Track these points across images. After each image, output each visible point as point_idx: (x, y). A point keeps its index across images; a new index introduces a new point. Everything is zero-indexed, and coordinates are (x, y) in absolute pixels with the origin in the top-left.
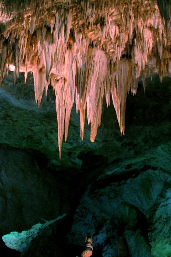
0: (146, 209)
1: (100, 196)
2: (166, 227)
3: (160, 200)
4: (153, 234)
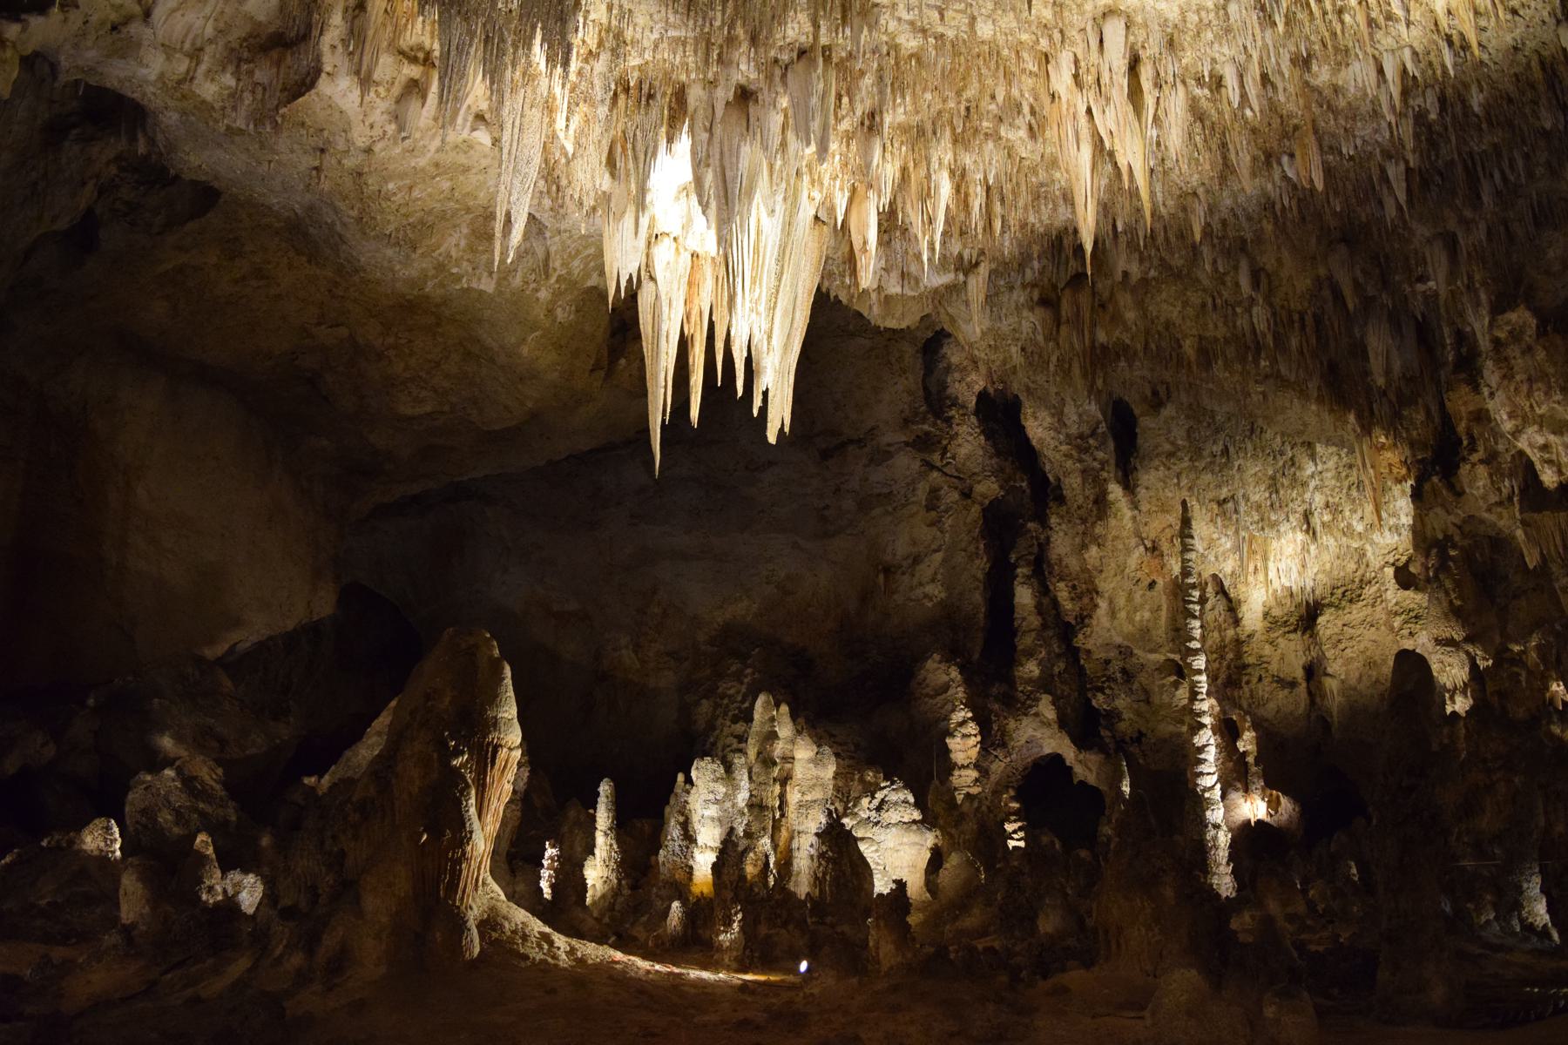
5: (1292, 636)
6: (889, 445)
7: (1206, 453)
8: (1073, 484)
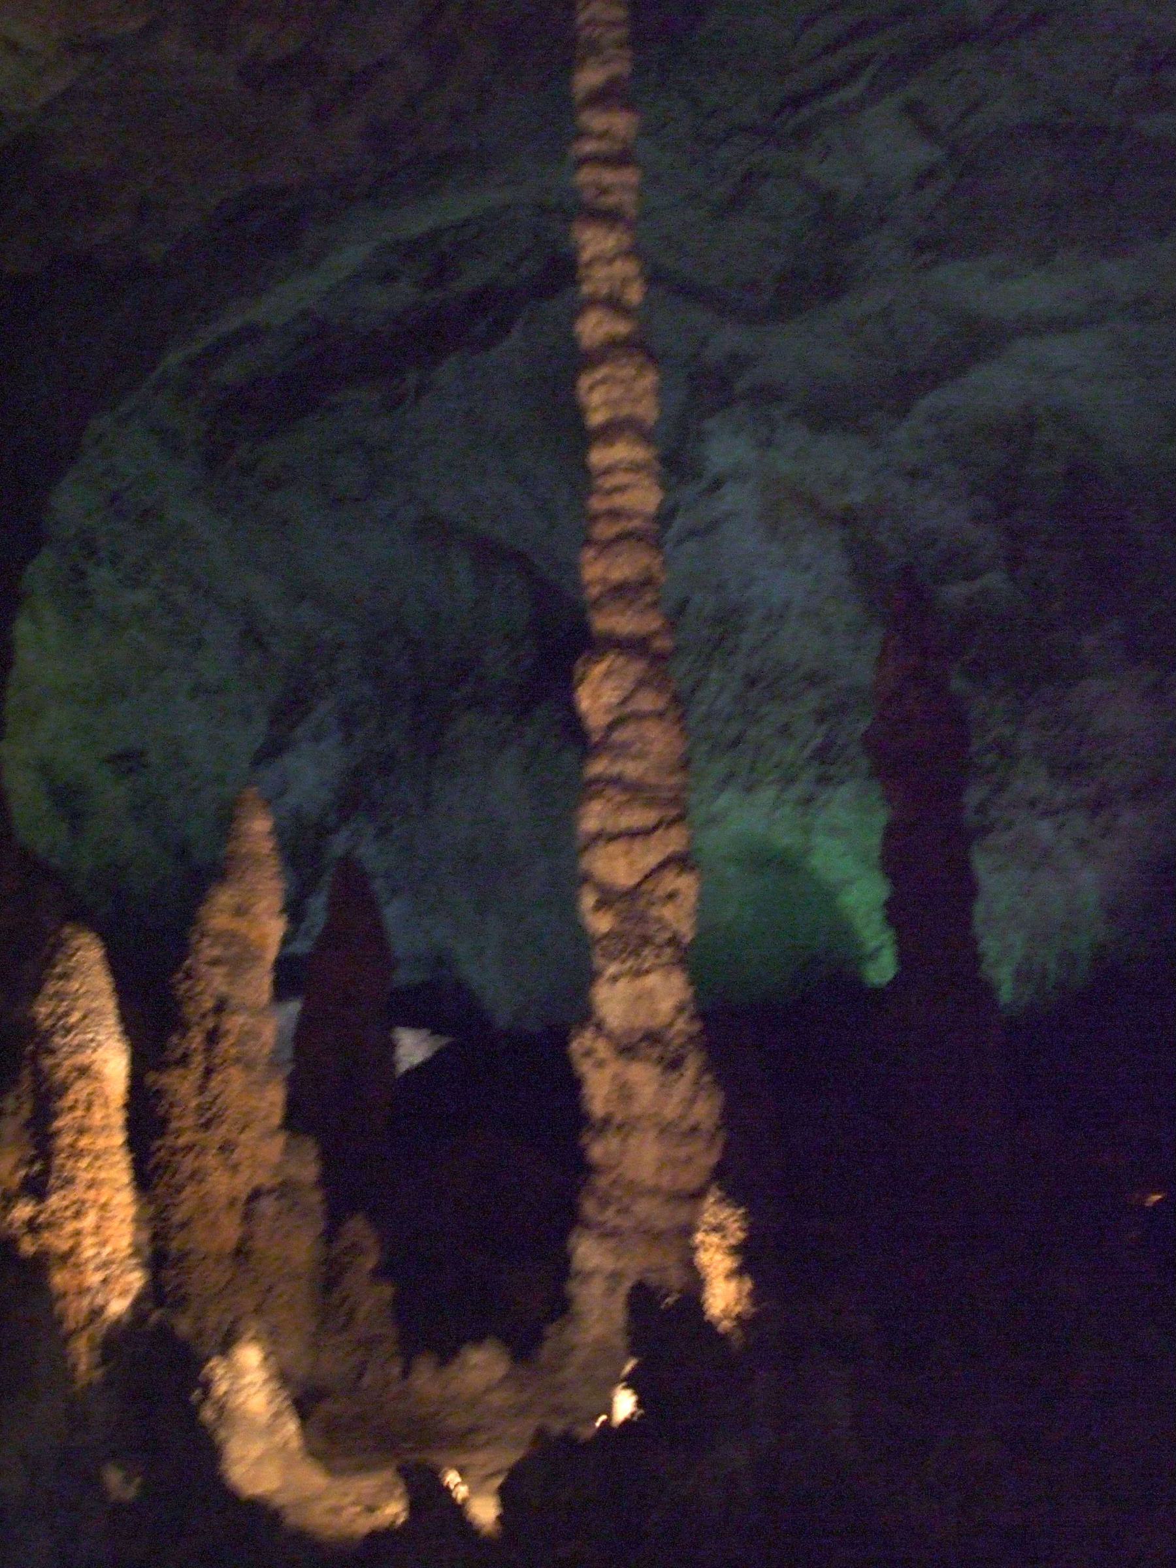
1: (273, 485)
2: (715, 675)
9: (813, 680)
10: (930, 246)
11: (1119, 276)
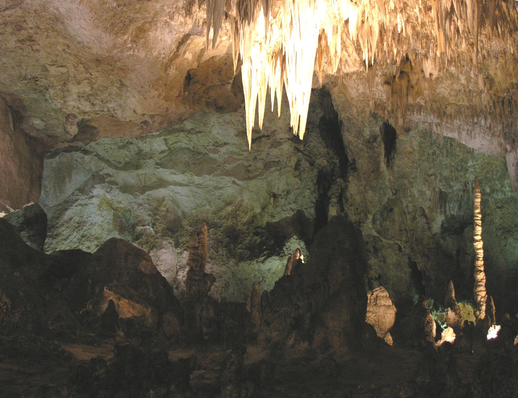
0: (51, 206)
2: (75, 233)
3: (78, 197)
4: (54, 241)
5: (452, 236)
6: (281, 139)
7: (426, 154)
8: (363, 163)
9: (97, 238)
10: (160, 165)
11: (197, 180)
